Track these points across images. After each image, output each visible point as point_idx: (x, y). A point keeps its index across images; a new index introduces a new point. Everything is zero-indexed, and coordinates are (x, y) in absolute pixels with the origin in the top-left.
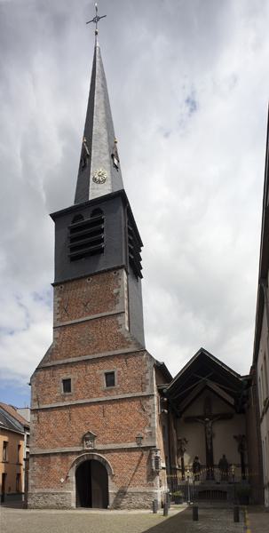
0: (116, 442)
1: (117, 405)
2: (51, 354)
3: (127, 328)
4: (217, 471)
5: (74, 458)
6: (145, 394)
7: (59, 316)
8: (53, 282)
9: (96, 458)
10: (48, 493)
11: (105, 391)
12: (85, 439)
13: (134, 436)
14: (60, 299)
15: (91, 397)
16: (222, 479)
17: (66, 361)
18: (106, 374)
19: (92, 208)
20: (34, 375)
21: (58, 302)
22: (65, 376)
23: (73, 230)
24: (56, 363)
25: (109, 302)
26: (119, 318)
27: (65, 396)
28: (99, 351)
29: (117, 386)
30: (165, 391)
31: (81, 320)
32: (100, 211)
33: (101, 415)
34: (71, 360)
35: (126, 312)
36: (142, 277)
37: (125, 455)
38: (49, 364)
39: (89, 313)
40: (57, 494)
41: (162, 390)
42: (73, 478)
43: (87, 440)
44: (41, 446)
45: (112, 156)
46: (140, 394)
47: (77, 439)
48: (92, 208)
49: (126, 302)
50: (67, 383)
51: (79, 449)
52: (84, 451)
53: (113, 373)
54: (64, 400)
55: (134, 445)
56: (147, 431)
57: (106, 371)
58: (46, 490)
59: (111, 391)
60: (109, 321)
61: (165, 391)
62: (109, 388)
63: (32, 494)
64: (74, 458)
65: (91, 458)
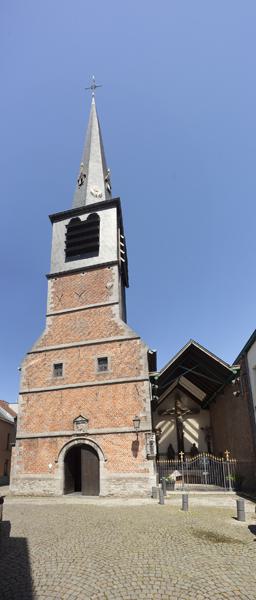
5: (64, 441)
9: (87, 442)
10: (35, 479)
11: (98, 376)
12: (75, 421)
22: (58, 362)
30: (156, 378)
36: (128, 286)
37: (117, 439)
40: (44, 479)
42: (61, 463)
43: (78, 423)
50: (58, 366)
52: (74, 435)
54: (53, 383)
57: (100, 356)
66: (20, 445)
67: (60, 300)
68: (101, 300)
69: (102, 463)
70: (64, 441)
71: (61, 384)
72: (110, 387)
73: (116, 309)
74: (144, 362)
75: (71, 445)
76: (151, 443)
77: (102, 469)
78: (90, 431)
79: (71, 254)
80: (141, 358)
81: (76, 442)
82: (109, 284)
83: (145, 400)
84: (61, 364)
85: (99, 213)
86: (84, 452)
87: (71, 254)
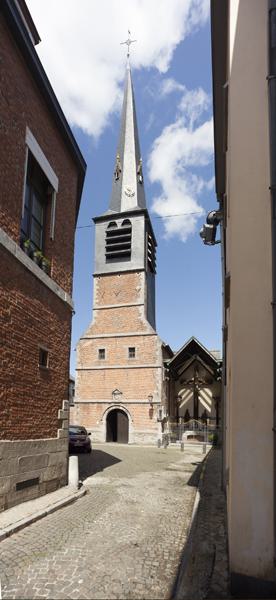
0: (135, 398)
5: (108, 406)
12: (113, 393)
22: (102, 348)
23: (109, 234)
29: (136, 358)
34: (106, 335)
37: (140, 407)
39: (119, 301)
42: (104, 422)
45: (138, 174)
47: (109, 393)
50: (102, 351)
55: (147, 401)
64: (108, 406)
68: (132, 300)
69: (130, 422)
72: (131, 372)
73: (142, 309)
74: (159, 353)
76: (161, 411)
77: (130, 426)
79: (110, 258)
82: (138, 288)
86: (119, 414)
87: (110, 258)
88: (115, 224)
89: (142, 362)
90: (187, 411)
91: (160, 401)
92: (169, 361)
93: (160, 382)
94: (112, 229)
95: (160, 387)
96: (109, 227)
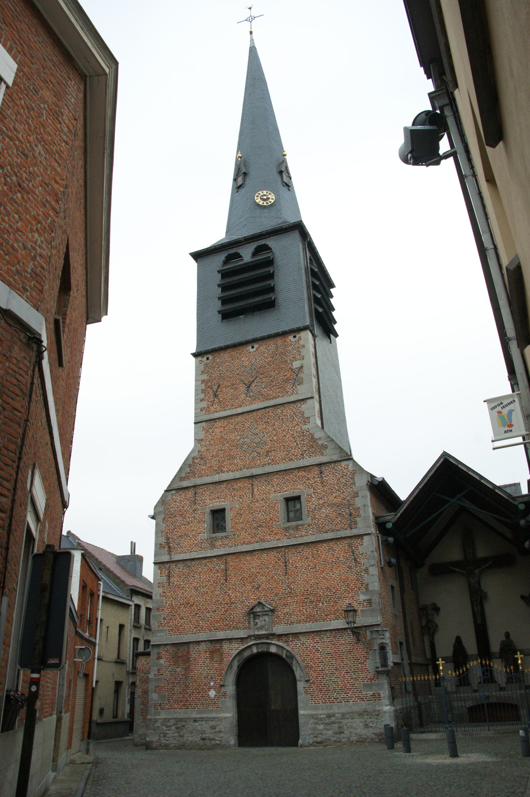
0: (310, 618)
1: (307, 552)
2: (190, 466)
3: (319, 423)
4: (498, 666)
6: (355, 532)
7: (204, 404)
8: (194, 351)
9: (273, 649)
11: (286, 529)
12: (252, 613)
13: (344, 604)
14: (205, 377)
15: (263, 541)
16: (509, 680)
17: (217, 478)
18: (288, 500)
19: (254, 245)
20: (163, 501)
21: (203, 381)
22: (217, 504)
23: (224, 274)
24: (199, 481)
25: (287, 381)
26: (304, 407)
27: (216, 539)
28: (274, 462)
29: (306, 520)
30: (389, 525)
31: (240, 410)
32: (266, 248)
33: (281, 571)
34: (224, 476)
35: (316, 396)
38: (185, 484)
39: (254, 399)
40: (202, 719)
41: (385, 523)
42: (231, 689)
43: (256, 616)
44: (177, 629)
46: (348, 533)
47: (240, 611)
48: (254, 245)
49: (314, 380)
51: (242, 634)
52: (249, 637)
53: (298, 498)
54: (213, 546)
55: (340, 624)
56: (362, 597)
58: (181, 714)
59: (297, 528)
60: (288, 411)
61: (389, 525)
62: (293, 524)
63: (156, 721)
65: (264, 649)
66: (159, 658)
67: (216, 396)
69: (301, 686)
70: (239, 647)
71: (224, 546)
75: (247, 654)
76: (382, 648)
77: (302, 697)
78: (278, 629)
80: (356, 495)
81: (255, 650)
82: (296, 365)
83: (366, 571)
84: (223, 510)
85: (270, 242)
88: (237, 256)
89: (320, 531)
90: (458, 640)
91: (378, 619)
92: (391, 518)
93: (374, 571)
94: (234, 264)
95: (375, 585)
96: (225, 263)
